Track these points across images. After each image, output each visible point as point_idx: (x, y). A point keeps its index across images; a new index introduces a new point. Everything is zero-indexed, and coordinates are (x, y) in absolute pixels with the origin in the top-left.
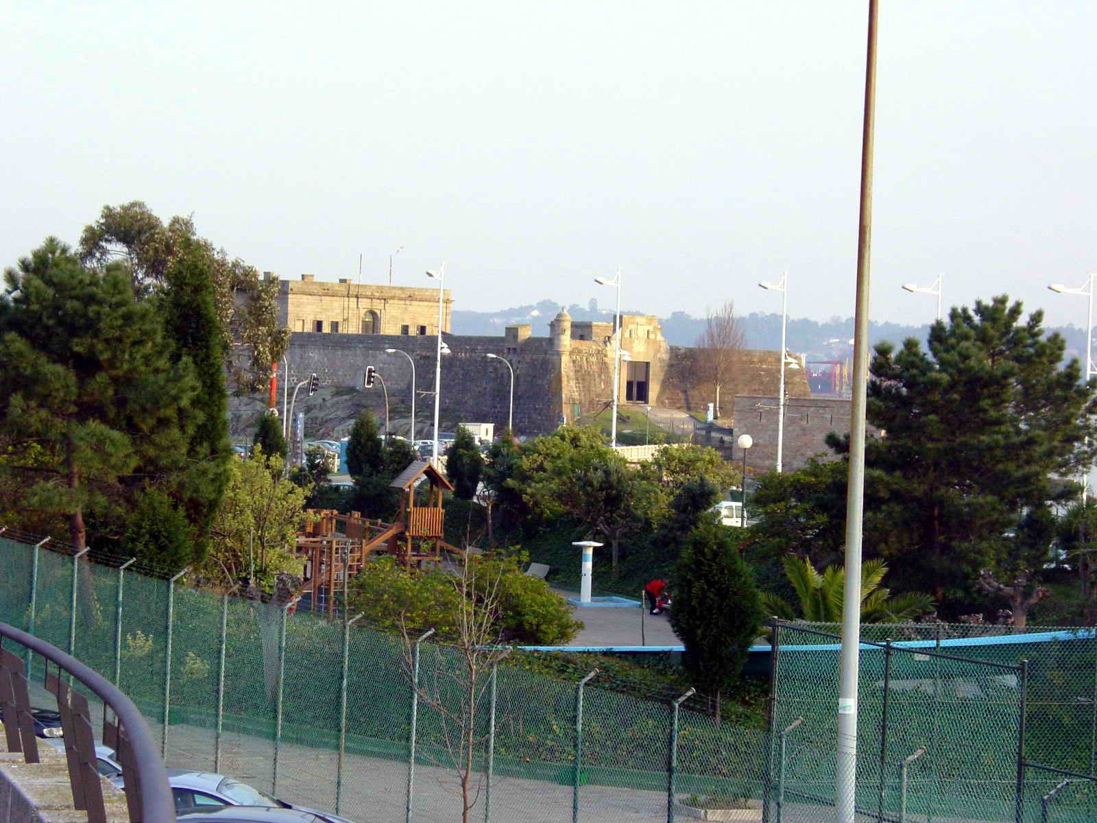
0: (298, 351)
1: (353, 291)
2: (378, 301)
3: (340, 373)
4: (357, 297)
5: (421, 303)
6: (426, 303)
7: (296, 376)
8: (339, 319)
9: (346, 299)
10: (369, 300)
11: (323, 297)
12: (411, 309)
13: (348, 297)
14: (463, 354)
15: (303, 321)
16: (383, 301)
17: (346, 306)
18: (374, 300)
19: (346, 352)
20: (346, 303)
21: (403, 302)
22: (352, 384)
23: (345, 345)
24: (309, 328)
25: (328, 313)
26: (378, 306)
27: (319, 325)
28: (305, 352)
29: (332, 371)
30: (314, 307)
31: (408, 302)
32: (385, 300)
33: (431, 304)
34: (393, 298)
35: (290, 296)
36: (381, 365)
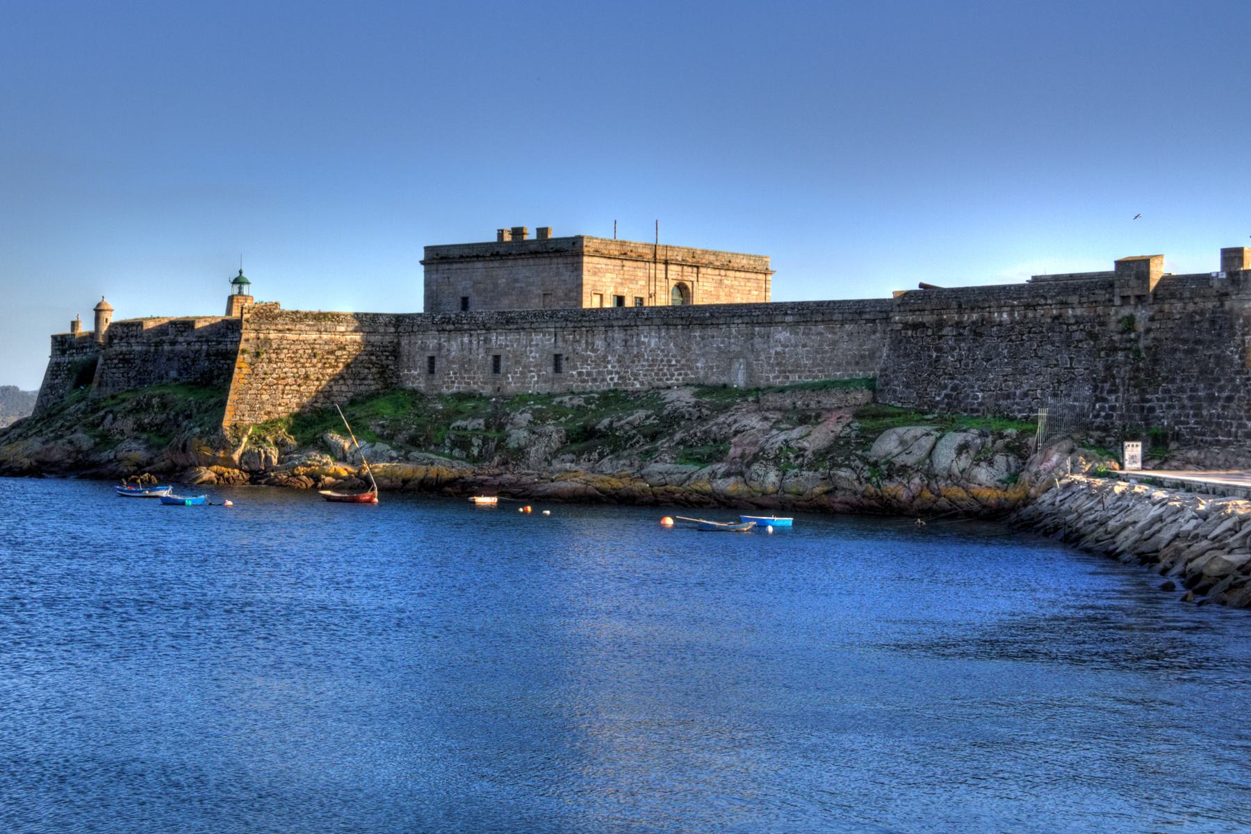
0: (618, 335)
1: (661, 255)
2: (690, 269)
3: (699, 365)
4: (666, 263)
5: (738, 274)
6: (743, 275)
7: (617, 373)
8: (644, 295)
9: (652, 265)
10: (679, 268)
11: (625, 263)
12: (726, 282)
13: (655, 263)
14: (1005, 316)
15: (601, 296)
16: (695, 269)
17: (652, 275)
18: (685, 268)
19: (709, 332)
20: (652, 272)
21: (717, 272)
22: (724, 379)
23: (709, 322)
24: (609, 304)
25: (631, 286)
26: (689, 275)
27: (620, 300)
28: (632, 336)
29: (683, 362)
30: (615, 276)
31: (723, 272)
32: (698, 267)
33: (748, 275)
34: (706, 266)
35: (586, 259)
36: (779, 349)
